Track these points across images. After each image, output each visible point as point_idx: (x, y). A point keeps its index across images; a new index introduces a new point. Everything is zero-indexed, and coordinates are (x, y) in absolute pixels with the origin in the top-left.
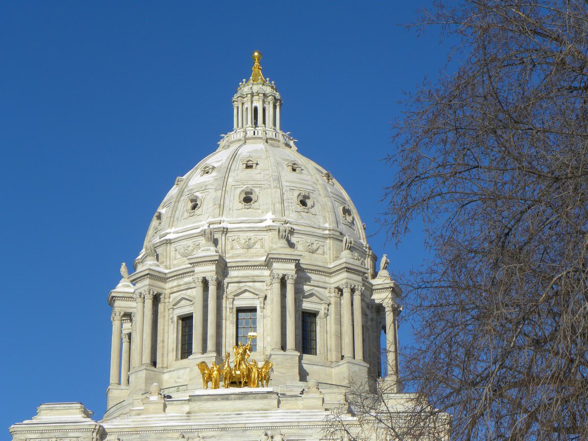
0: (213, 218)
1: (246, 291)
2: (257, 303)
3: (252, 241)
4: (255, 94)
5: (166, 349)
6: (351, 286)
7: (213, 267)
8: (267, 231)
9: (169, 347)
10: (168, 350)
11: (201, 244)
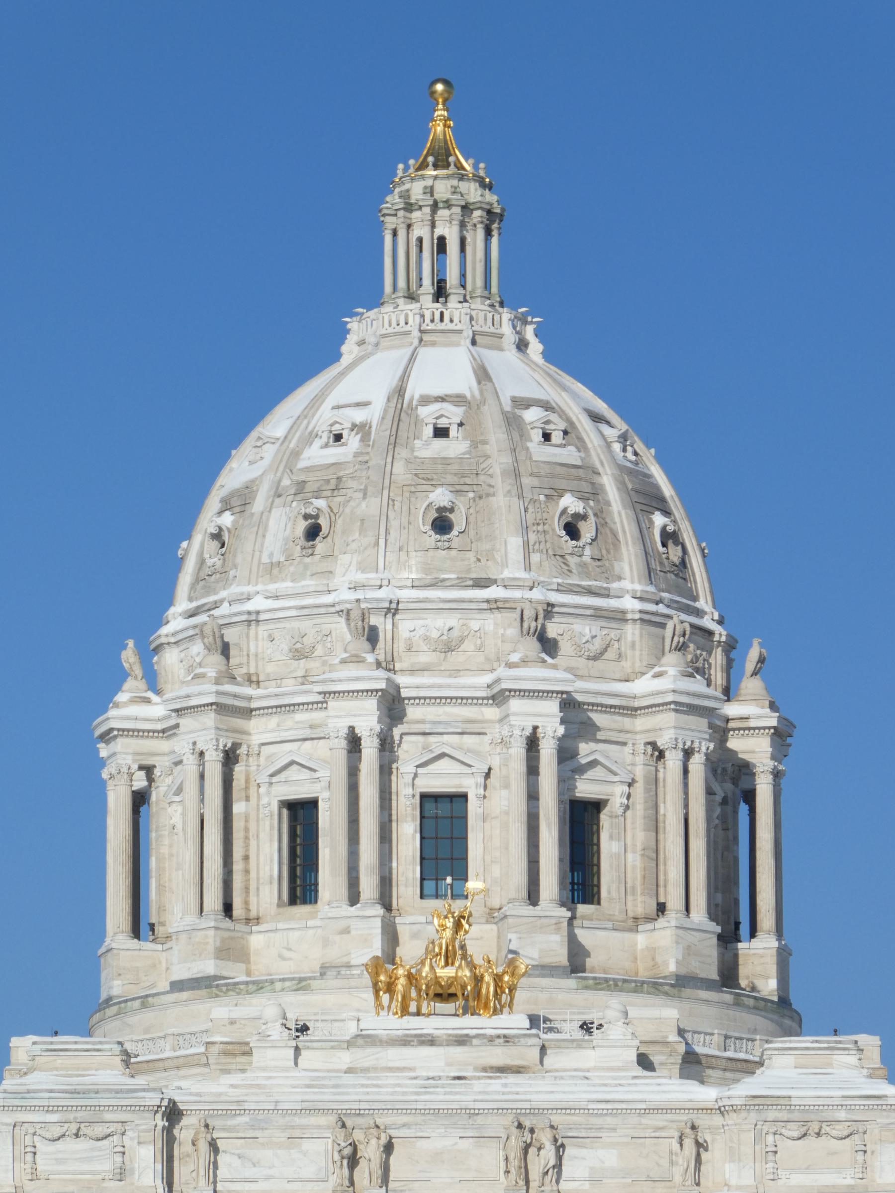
0: (363, 572)
1: (443, 755)
2: (470, 786)
3: (455, 634)
4: (441, 205)
5: (253, 875)
6: (684, 744)
7: (371, 704)
8: (491, 609)
9: (261, 872)
10: (258, 879)
11: (334, 634)
